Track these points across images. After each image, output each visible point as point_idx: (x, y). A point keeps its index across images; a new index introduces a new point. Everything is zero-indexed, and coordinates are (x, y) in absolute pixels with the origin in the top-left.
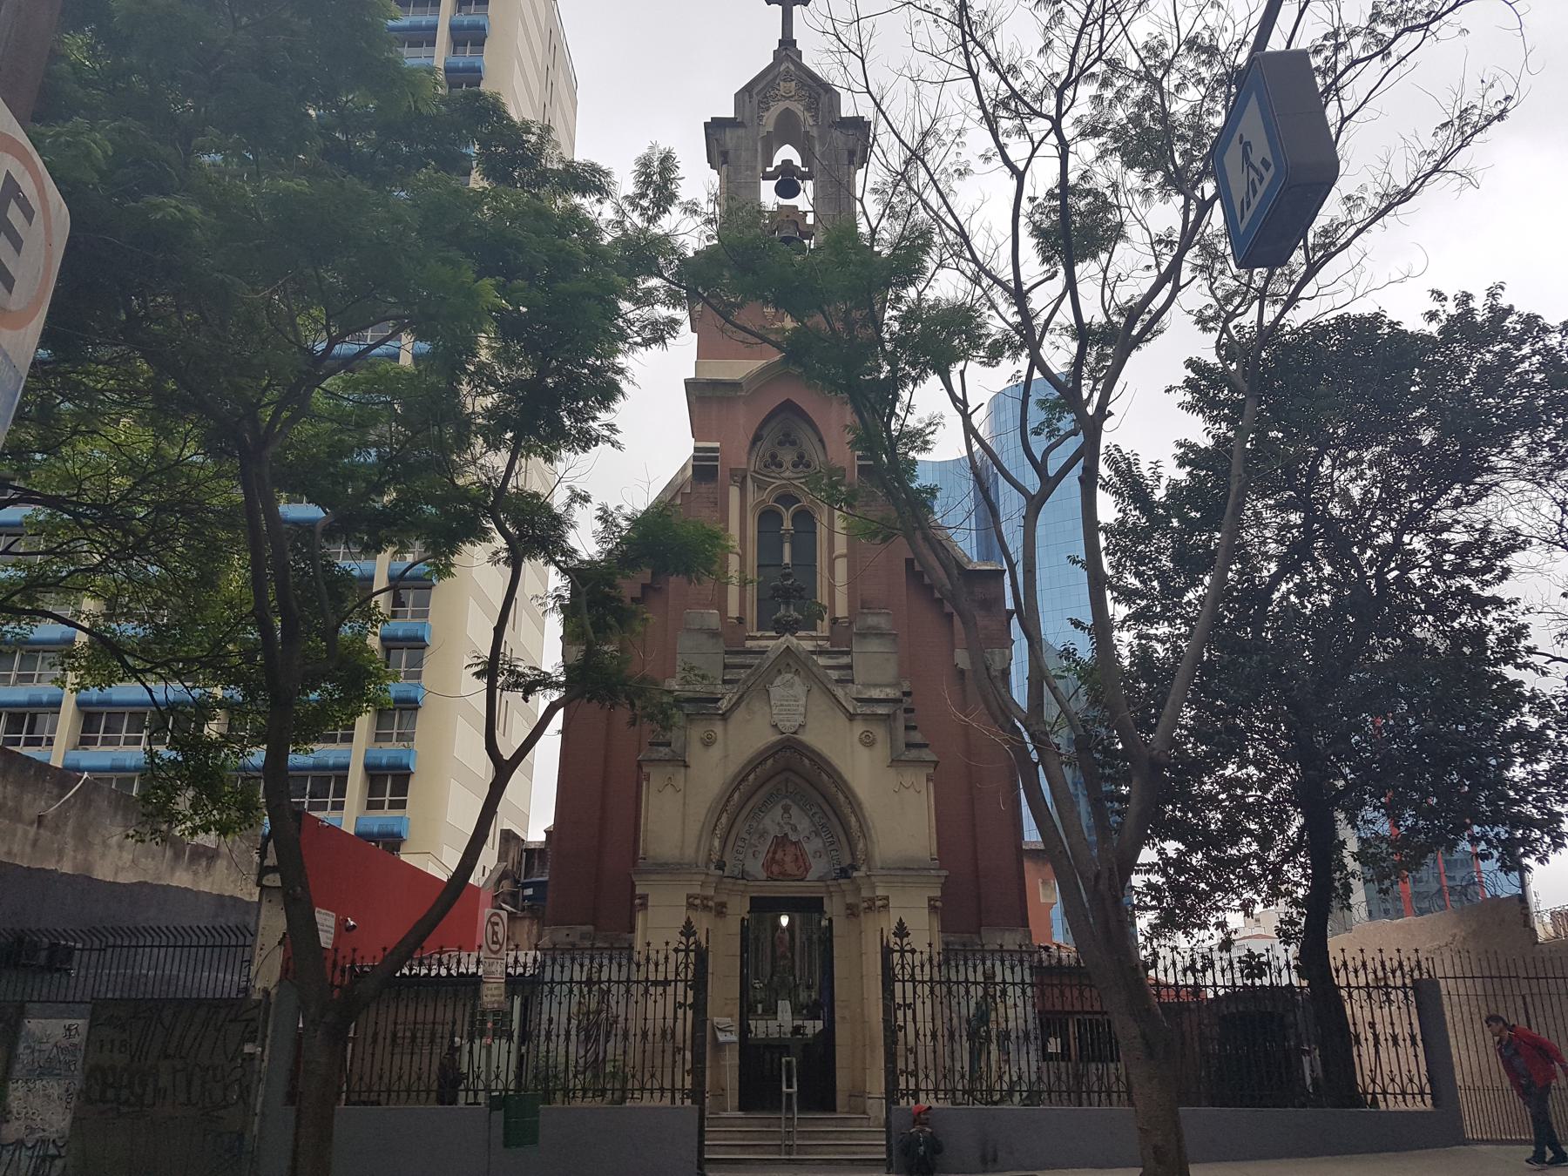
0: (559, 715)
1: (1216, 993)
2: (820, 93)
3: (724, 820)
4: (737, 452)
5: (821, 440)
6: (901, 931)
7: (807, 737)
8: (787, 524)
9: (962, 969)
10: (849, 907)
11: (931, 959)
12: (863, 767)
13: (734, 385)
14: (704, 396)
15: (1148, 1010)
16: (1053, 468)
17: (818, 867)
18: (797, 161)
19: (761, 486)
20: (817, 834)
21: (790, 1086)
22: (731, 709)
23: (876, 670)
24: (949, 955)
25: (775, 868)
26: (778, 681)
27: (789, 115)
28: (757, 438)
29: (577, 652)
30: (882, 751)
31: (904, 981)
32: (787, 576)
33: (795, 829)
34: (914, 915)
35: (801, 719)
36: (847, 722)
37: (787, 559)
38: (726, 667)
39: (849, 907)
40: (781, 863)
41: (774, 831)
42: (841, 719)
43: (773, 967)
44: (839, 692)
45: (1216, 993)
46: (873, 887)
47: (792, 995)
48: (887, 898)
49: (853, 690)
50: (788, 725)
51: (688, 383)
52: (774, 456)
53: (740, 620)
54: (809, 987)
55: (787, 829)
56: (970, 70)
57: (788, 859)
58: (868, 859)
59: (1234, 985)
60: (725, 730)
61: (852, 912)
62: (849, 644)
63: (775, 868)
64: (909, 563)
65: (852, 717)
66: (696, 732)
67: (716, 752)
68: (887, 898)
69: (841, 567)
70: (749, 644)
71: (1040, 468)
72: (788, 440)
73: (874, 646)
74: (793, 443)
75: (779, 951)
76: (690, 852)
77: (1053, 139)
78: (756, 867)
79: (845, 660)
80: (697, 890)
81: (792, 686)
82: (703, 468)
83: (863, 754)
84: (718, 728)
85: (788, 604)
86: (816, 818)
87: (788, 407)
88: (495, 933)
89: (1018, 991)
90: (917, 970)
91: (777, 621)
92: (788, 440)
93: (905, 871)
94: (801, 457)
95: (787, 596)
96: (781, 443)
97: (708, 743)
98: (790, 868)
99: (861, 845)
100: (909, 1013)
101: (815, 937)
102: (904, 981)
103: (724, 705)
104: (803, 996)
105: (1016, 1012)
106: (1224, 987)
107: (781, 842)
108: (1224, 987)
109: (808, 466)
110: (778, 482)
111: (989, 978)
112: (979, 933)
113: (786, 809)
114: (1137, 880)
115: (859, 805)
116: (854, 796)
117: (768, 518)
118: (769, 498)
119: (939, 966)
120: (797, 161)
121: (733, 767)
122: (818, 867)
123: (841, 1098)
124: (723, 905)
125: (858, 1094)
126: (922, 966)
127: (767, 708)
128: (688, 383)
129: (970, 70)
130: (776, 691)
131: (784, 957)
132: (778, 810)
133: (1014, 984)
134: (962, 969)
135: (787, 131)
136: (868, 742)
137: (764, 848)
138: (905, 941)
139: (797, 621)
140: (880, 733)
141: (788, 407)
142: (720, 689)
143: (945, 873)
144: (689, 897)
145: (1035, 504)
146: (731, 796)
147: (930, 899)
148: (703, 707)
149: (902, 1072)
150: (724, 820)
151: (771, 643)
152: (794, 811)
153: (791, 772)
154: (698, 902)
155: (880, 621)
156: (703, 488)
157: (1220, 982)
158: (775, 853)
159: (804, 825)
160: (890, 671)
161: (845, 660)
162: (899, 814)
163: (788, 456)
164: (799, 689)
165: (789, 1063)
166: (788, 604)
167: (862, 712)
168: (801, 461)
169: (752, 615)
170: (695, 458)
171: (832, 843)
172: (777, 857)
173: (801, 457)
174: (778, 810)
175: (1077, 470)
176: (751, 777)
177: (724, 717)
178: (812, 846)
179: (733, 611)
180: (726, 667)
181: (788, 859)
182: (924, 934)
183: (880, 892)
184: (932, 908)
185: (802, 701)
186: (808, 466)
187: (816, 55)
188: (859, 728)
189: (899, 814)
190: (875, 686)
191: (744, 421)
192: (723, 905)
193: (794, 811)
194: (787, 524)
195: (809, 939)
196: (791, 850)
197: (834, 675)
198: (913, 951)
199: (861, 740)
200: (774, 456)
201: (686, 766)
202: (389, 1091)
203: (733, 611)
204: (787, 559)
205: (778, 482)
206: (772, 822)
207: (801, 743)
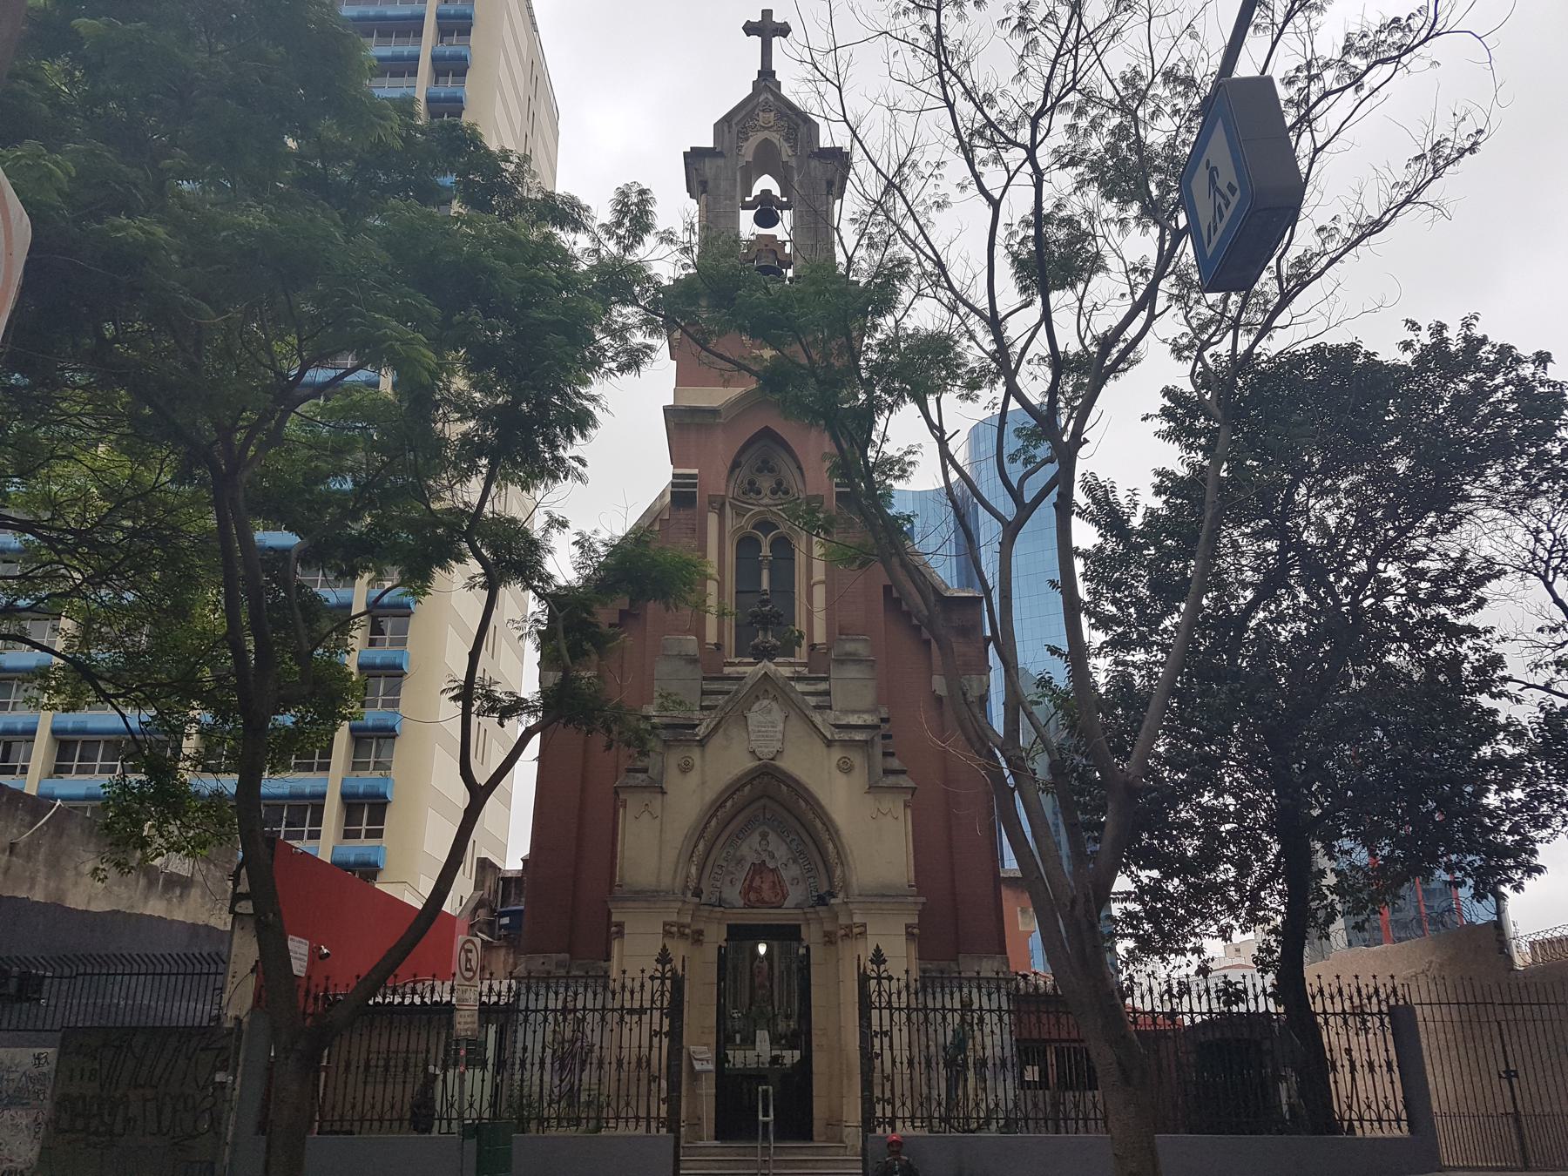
0: (536, 740)
1: (1192, 1020)
2: (798, 123)
3: (701, 846)
4: (715, 479)
5: (800, 468)
6: (878, 958)
7: (784, 764)
8: (766, 551)
9: (939, 996)
10: (826, 934)
11: (907, 986)
12: (840, 793)
13: (714, 412)
14: (679, 420)
15: (1124, 1037)
16: (1028, 498)
17: (795, 895)
18: (776, 191)
19: (740, 514)
21: (766, 1114)
22: (708, 736)
23: (854, 697)
24: (927, 982)
25: (752, 896)
26: (756, 707)
27: (767, 147)
28: (736, 465)
29: (554, 677)
30: (859, 778)
31: (880, 1009)
32: (765, 603)
34: (892, 944)
35: (778, 746)
37: (765, 585)
38: (704, 693)
40: (758, 891)
41: (751, 858)
42: (819, 746)
43: (752, 998)
44: (817, 718)
45: (1192, 1020)
46: (851, 915)
47: (770, 1024)
48: (864, 925)
49: (831, 716)
50: (766, 751)
51: (666, 410)
52: (752, 483)
53: (719, 646)
54: (788, 1017)
56: (946, 99)
58: (846, 886)
59: (1210, 1011)
60: (703, 757)
61: (830, 939)
62: (828, 671)
64: (887, 590)
65: (829, 743)
66: (674, 759)
67: (693, 778)
68: (864, 925)
69: (819, 593)
70: (727, 670)
71: (1016, 494)
72: (766, 467)
73: (852, 672)
74: (771, 470)
75: (757, 981)
76: (666, 881)
77: (1028, 168)
78: (733, 894)
79: (822, 686)
80: (674, 918)
81: (770, 712)
82: (681, 495)
83: (841, 780)
84: (696, 754)
85: (766, 631)
86: (794, 846)
87: (767, 434)
88: (468, 960)
89: (995, 1018)
90: (894, 997)
91: (756, 647)
92: (766, 467)
93: (883, 897)
94: (779, 484)
95: (765, 621)
96: (760, 470)
97: (685, 769)
98: (767, 894)
99: (838, 872)
100: (886, 1040)
101: (794, 966)
102: (880, 1009)
103: (701, 731)
104: (782, 1026)
105: (994, 1039)
106: (1201, 1013)
107: (759, 869)
108: (1201, 1013)
109: (786, 492)
110: (757, 509)
111: (966, 1006)
112: (956, 960)
113: (764, 836)
114: (1116, 909)
115: (837, 832)
116: (830, 820)
117: (747, 545)
118: (746, 523)
119: (916, 993)
120: (776, 191)
121: (710, 795)
122: (795, 895)
123: (818, 1126)
124: (700, 933)
125: (835, 1123)
126: (899, 993)
128: (666, 410)
129: (946, 99)
130: (754, 717)
131: (762, 986)
132: (756, 837)
133: (991, 1011)
134: (939, 996)
135: (766, 161)
136: (846, 768)
138: (882, 968)
139: (774, 647)
140: (857, 759)
141: (767, 434)
142: (697, 714)
143: (923, 899)
144: (665, 924)
145: (1011, 530)
146: (708, 822)
147: (907, 926)
148: (681, 733)
149: (878, 1100)
150: (701, 846)
151: (749, 669)
152: (772, 837)
153: (770, 798)
154: (675, 929)
155: (860, 648)
156: (682, 514)
157: (1196, 1009)
159: (782, 852)
160: (868, 697)
161: (822, 686)
162: (876, 841)
163: (766, 483)
164: (777, 714)
165: (765, 1092)
166: (766, 631)
167: (840, 740)
168: (779, 488)
169: (730, 641)
170: (673, 484)
173: (779, 484)
174: (756, 837)
175: (1053, 496)
176: (729, 804)
177: (702, 743)
178: (790, 873)
179: (711, 636)
180: (704, 693)
181: (765, 886)
182: (901, 960)
183: (857, 919)
184: (910, 935)
185: (780, 727)
186: (786, 492)
187: (794, 85)
188: (837, 754)
189: (876, 841)
190: (854, 712)
191: (723, 448)
192: (700, 933)
193: (772, 837)
194: (766, 551)
195: (789, 968)
197: (812, 701)
198: (890, 978)
199: (838, 766)
200: (752, 483)
201: (664, 793)
202: (362, 1120)
203: (711, 636)
204: (765, 585)
205: (757, 509)
206: (750, 849)
207: (777, 768)
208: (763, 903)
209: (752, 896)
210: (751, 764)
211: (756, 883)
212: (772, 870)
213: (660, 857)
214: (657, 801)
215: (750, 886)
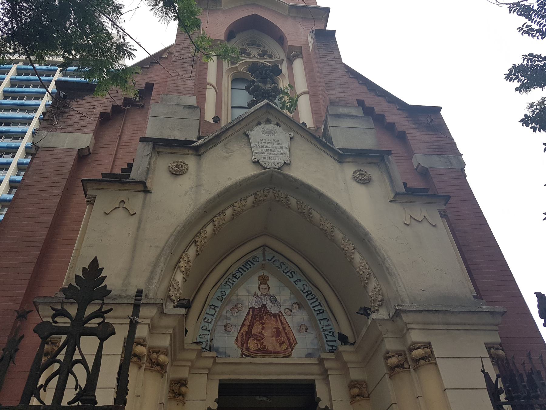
10: (353, 385)
17: (305, 343)
20: (300, 306)
33: (274, 300)
35: (285, 159)
36: (337, 165)
39: (353, 385)
40: (259, 338)
46: (402, 334)
48: (428, 345)
50: (272, 161)
55: (265, 300)
57: (268, 333)
63: (252, 344)
67: (186, 182)
68: (428, 345)
74: (259, 45)
78: (228, 342)
83: (360, 190)
97: (177, 172)
98: (270, 343)
107: (259, 314)
113: (263, 280)
122: (305, 343)
124: (182, 383)
127: (248, 150)
136: (363, 180)
137: (238, 321)
147: (489, 347)
152: (272, 282)
158: (251, 326)
159: (285, 297)
171: (321, 312)
172: (255, 331)
178: (295, 319)
181: (268, 333)
183: (416, 336)
192: (182, 383)
196: (271, 325)
199: (355, 178)
201: (147, 191)
206: (248, 294)
208: (265, 352)
209: (252, 344)
210: (252, 171)
211: (256, 329)
212: (275, 315)
213: (133, 258)
214: (136, 201)
215: (249, 332)
